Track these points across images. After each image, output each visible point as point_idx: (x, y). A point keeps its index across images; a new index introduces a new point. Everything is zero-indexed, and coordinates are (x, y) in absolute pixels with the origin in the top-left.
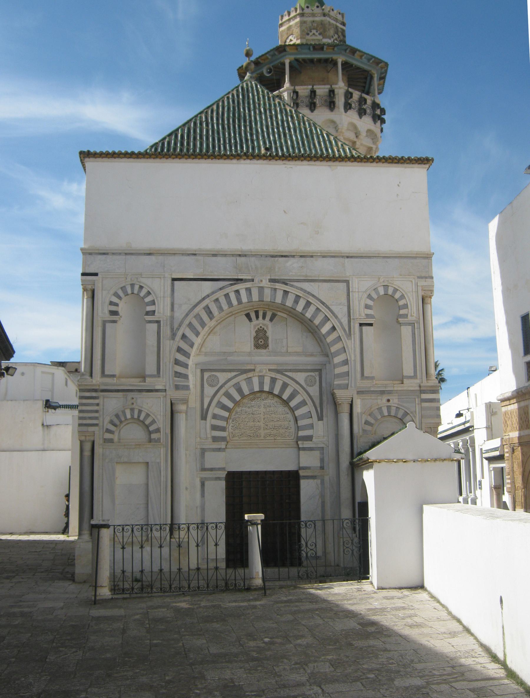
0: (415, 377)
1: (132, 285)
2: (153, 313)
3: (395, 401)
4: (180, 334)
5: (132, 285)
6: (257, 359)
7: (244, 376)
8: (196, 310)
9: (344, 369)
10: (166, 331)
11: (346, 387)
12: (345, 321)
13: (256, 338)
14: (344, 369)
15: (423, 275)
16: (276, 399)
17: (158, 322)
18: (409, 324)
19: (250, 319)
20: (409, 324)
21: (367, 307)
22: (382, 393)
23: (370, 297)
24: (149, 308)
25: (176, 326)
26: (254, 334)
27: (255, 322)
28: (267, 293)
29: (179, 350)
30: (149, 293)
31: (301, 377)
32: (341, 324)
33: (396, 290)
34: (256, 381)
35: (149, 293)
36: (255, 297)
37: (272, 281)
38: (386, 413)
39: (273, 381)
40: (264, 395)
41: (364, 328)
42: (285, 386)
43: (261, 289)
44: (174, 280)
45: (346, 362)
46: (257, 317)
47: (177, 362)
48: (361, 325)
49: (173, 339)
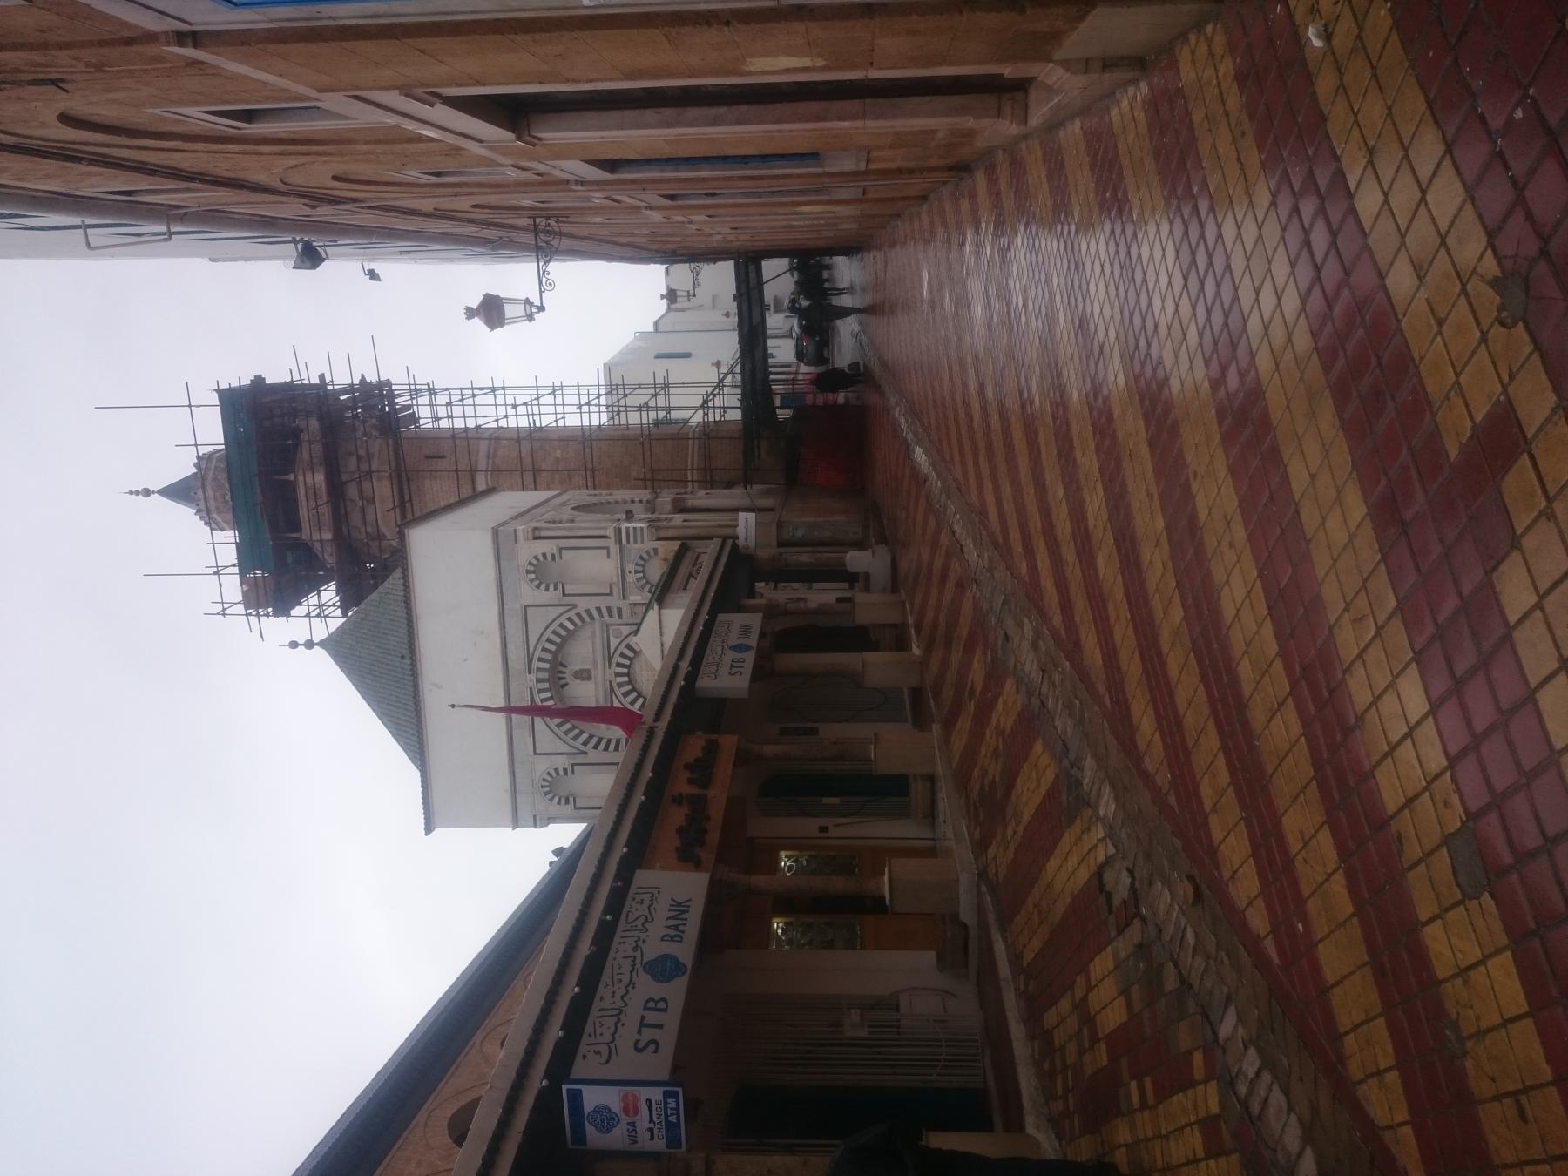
0: (607, 548)
1: (543, 787)
2: (565, 771)
3: (630, 567)
4: (583, 748)
5: (543, 787)
6: (600, 679)
7: (616, 688)
8: (563, 735)
9: (604, 611)
10: (580, 759)
11: (620, 610)
12: (562, 609)
13: (583, 679)
14: (604, 611)
15: (513, 537)
16: (634, 661)
17: (573, 765)
18: (560, 552)
19: (566, 684)
20: (560, 552)
21: (547, 589)
22: (623, 578)
23: (538, 587)
24: (561, 773)
25: (575, 751)
26: (579, 681)
27: (568, 680)
28: (541, 675)
29: (596, 747)
30: (549, 774)
31: (614, 642)
32: (566, 612)
33: (530, 564)
34: (620, 680)
35: (549, 774)
36: (546, 685)
37: (530, 673)
38: (641, 575)
39: (619, 665)
40: (632, 671)
41: (567, 592)
42: (623, 655)
43: (539, 680)
44: (535, 753)
45: (599, 610)
46: (564, 678)
47: (606, 748)
48: (564, 595)
49: (586, 753)
